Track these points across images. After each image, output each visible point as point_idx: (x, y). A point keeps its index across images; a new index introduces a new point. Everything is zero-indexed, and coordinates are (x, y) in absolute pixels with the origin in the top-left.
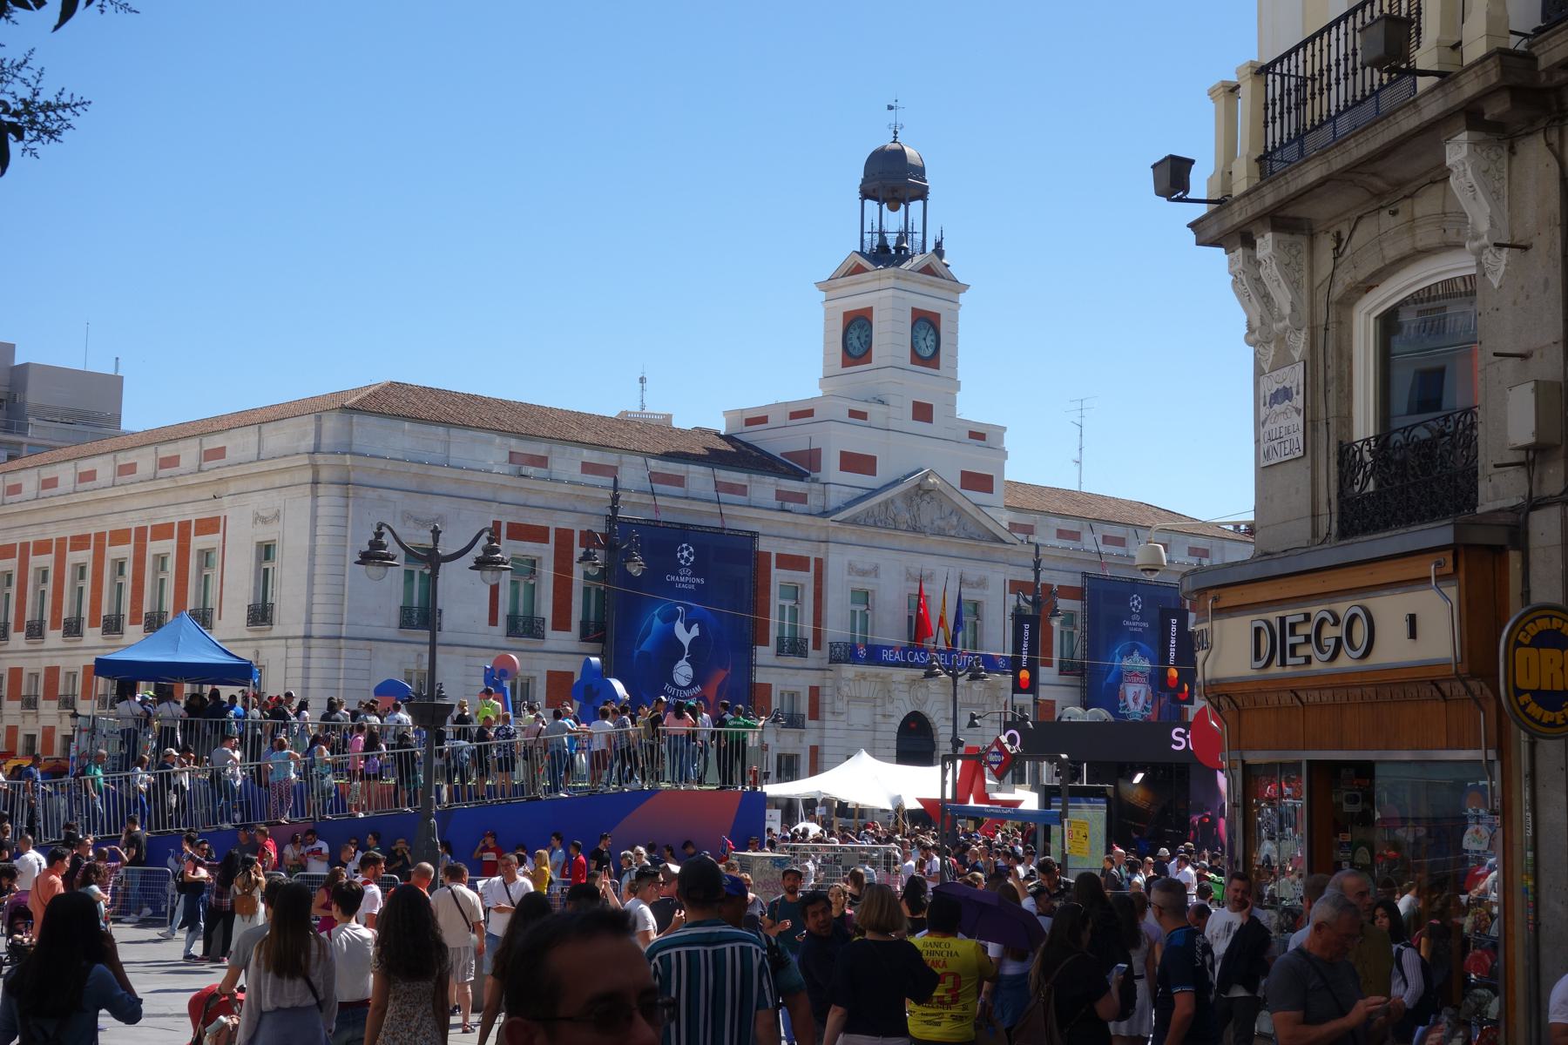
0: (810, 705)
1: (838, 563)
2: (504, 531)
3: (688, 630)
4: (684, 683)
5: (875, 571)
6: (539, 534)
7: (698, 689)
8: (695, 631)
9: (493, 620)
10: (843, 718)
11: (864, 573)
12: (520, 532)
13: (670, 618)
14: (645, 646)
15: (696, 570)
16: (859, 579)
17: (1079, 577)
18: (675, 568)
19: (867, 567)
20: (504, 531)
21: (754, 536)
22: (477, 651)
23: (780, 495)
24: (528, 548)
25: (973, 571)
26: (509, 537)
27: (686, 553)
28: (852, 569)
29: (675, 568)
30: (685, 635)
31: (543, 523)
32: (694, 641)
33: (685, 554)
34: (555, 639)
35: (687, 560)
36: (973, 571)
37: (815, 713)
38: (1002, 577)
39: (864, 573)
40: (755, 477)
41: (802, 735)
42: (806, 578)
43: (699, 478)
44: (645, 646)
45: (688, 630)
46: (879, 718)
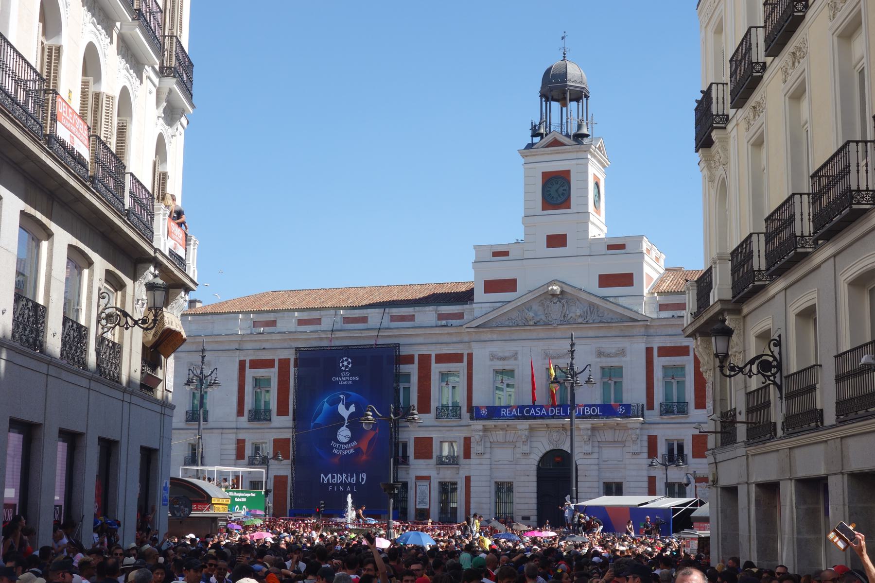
0: (465, 449)
1: (482, 355)
2: (247, 365)
3: (347, 408)
4: (345, 440)
5: (515, 356)
6: (269, 364)
7: (355, 443)
8: (352, 408)
9: (240, 413)
10: (487, 456)
11: (504, 359)
12: (256, 364)
13: (335, 403)
14: (318, 420)
15: (352, 372)
16: (501, 363)
17: (293, 351)
18: (338, 372)
19: (507, 354)
20: (247, 365)
21: (398, 346)
22: (431, 429)
23: (441, 317)
24: (261, 372)
25: (610, 345)
26: (251, 367)
27: (346, 363)
28: (493, 357)
29: (338, 372)
30: (344, 412)
31: (271, 357)
32: (351, 416)
33: (345, 363)
34: (278, 421)
35: (346, 367)
36: (610, 345)
37: (467, 455)
38: (643, 347)
39: (504, 359)
40: (417, 308)
41: (458, 469)
42: (462, 367)
43: (375, 316)
44: (318, 420)
45: (347, 408)
46: (518, 456)
